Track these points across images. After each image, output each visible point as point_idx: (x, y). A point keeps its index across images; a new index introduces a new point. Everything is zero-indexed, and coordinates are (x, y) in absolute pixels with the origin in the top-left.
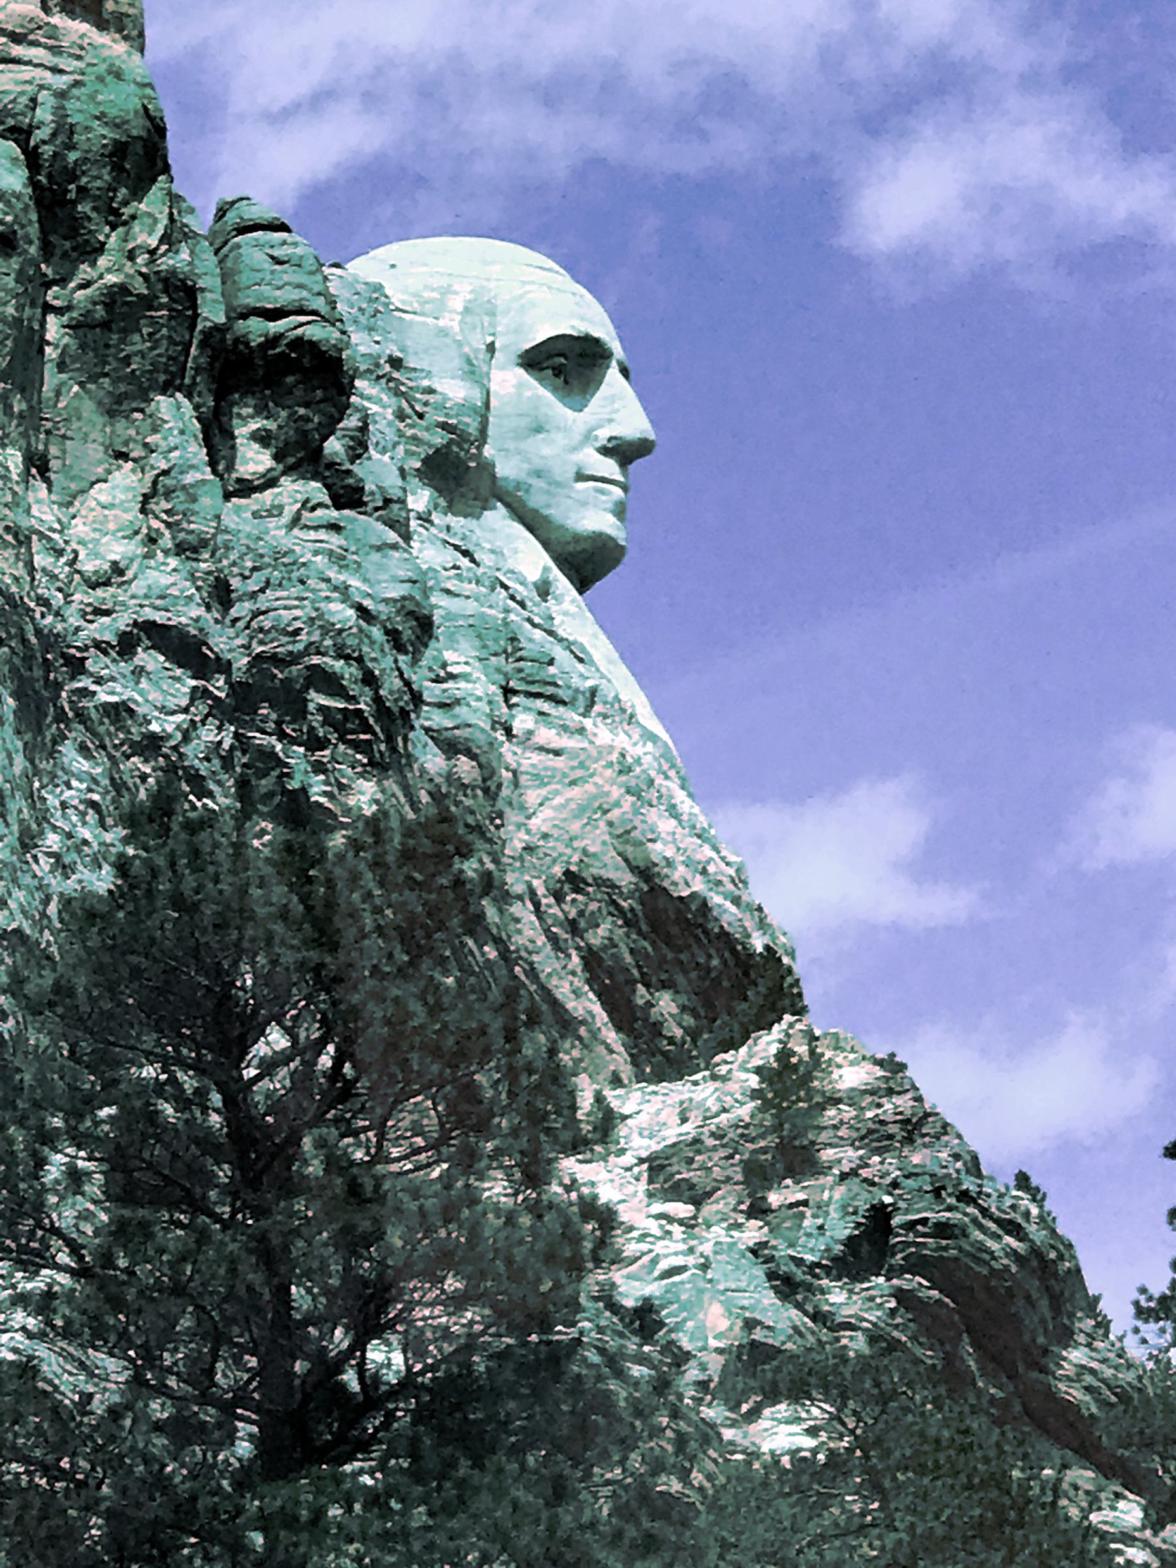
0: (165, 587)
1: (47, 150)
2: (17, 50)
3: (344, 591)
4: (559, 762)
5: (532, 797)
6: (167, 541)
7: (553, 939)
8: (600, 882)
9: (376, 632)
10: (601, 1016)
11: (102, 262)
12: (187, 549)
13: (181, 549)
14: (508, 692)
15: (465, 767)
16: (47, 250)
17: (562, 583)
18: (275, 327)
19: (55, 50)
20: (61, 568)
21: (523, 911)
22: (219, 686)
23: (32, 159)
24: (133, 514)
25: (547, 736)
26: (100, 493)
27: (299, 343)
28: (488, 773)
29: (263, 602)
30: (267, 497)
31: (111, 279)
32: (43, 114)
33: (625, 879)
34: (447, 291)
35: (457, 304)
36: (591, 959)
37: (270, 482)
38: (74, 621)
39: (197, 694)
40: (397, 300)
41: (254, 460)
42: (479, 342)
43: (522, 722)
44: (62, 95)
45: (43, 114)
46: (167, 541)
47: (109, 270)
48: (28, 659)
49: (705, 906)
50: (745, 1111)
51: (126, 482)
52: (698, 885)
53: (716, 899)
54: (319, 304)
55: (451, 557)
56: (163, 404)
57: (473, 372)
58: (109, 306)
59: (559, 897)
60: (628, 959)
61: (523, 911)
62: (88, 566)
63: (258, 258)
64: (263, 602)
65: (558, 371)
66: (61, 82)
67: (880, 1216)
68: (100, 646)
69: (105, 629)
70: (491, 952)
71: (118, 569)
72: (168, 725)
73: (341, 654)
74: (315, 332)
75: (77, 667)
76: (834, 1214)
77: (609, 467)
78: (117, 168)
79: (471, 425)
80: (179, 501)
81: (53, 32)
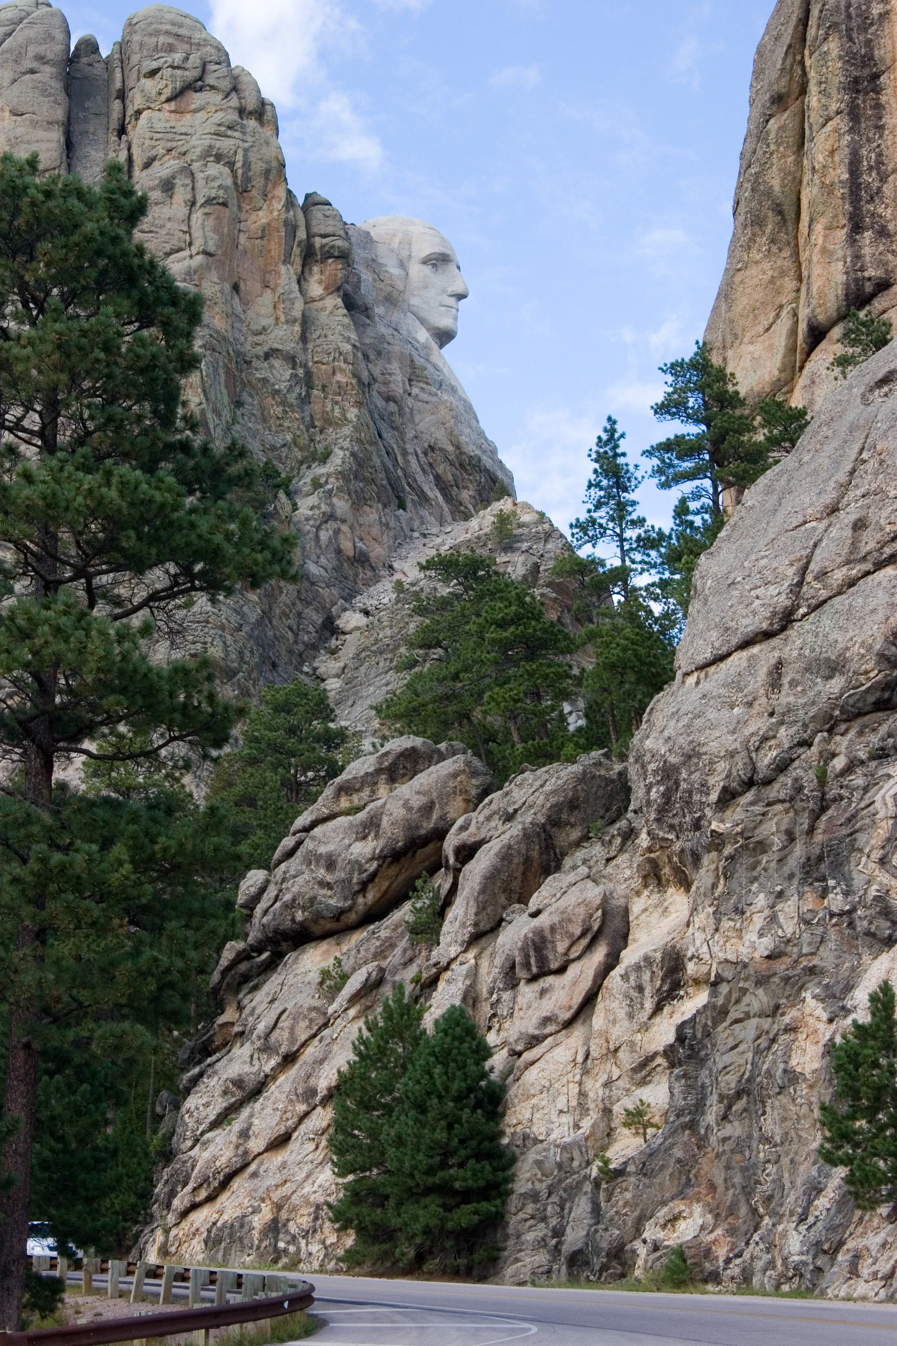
0: (284, 336)
1: (240, 172)
2: (229, 133)
3: (348, 340)
4: (428, 407)
5: (417, 418)
6: (283, 319)
7: (423, 470)
8: (441, 449)
9: (360, 355)
10: (440, 498)
11: (261, 213)
12: (291, 322)
13: (287, 322)
14: (410, 380)
15: (392, 407)
16: (240, 208)
17: (434, 346)
18: (324, 241)
19: (244, 133)
20: (245, 329)
21: (412, 459)
22: (301, 372)
23: (234, 172)
24: (271, 309)
25: (423, 396)
26: (259, 300)
27: (333, 247)
28: (401, 409)
29: (318, 342)
30: (319, 305)
31: (264, 221)
32: (239, 157)
33: (451, 448)
34: (394, 235)
35: (397, 240)
36: (438, 478)
37: (322, 299)
38: (248, 347)
39: (294, 376)
40: (375, 238)
41: (315, 289)
42: (405, 254)
43: (415, 391)
44: (246, 150)
45: (239, 157)
46: (283, 319)
47: (262, 217)
48: (230, 361)
49: (480, 460)
50: (487, 530)
51: (268, 297)
52: (478, 452)
53: (484, 458)
54: (342, 233)
55: (390, 331)
56: (283, 269)
57: (402, 265)
58: (263, 230)
59: (426, 454)
60: (450, 478)
61: (412, 459)
62: (254, 327)
63: (319, 215)
64: (318, 342)
65: (434, 265)
66: (246, 145)
67: (536, 566)
68: (258, 357)
69: (260, 351)
70: (400, 473)
71: (264, 329)
72: (283, 386)
73: (345, 361)
74: (339, 243)
75: (248, 363)
76: (519, 566)
77: (452, 301)
78: (267, 179)
79: (400, 285)
80: (288, 304)
81: (243, 127)
